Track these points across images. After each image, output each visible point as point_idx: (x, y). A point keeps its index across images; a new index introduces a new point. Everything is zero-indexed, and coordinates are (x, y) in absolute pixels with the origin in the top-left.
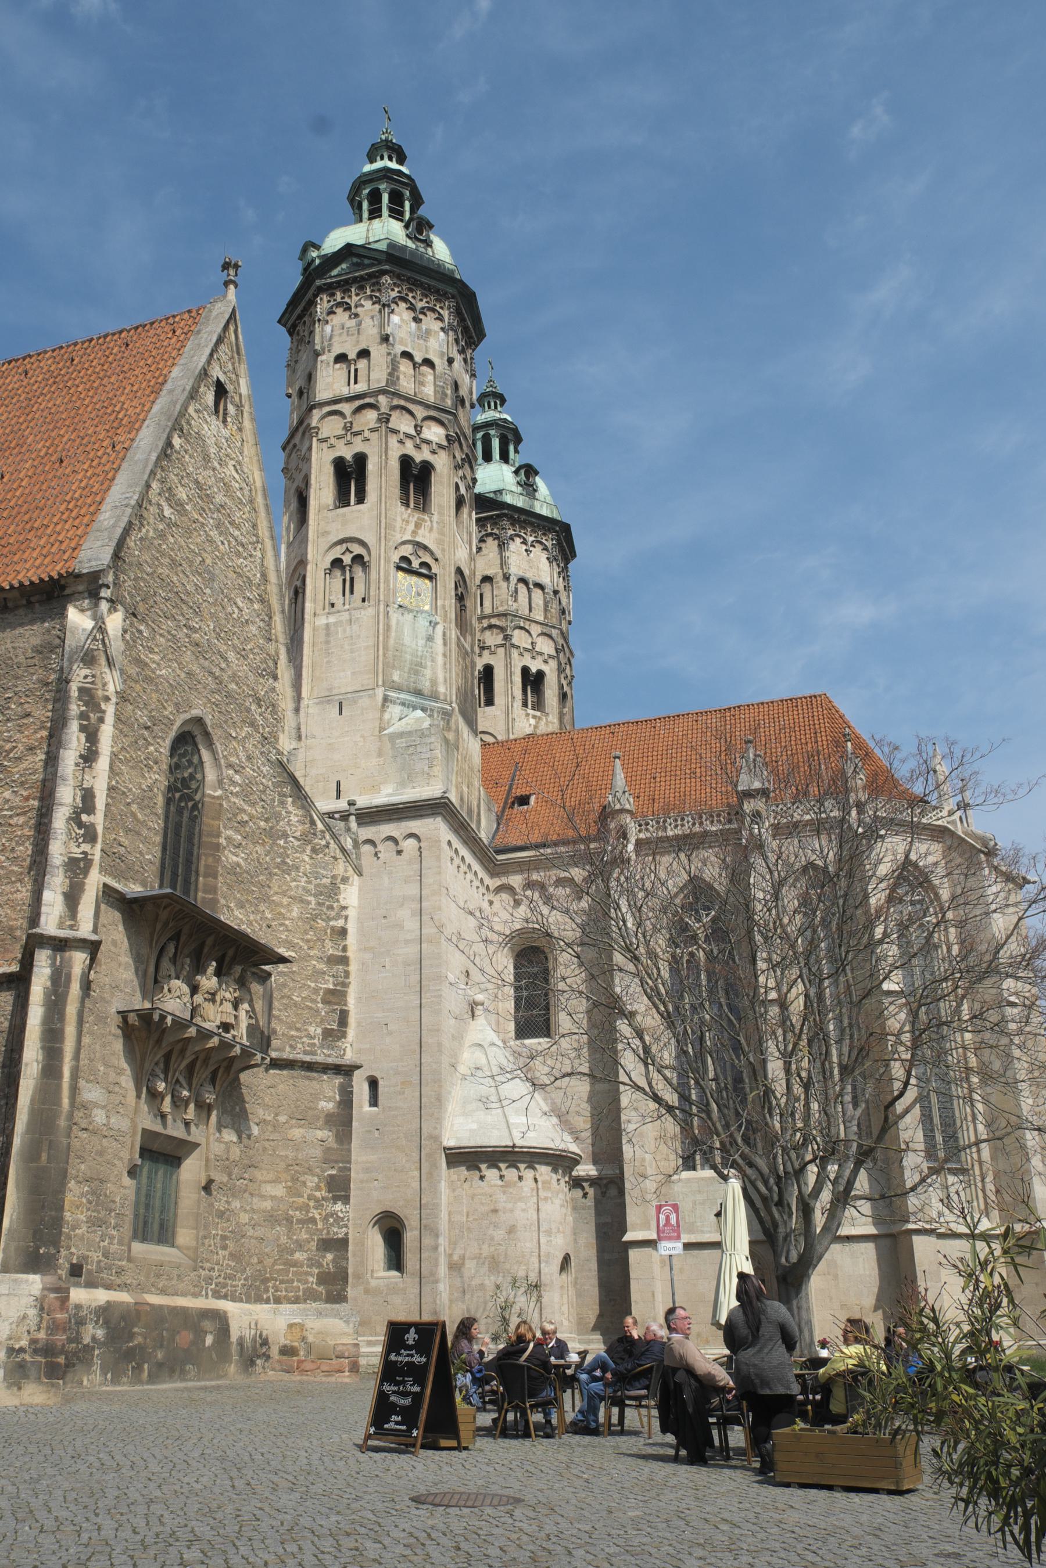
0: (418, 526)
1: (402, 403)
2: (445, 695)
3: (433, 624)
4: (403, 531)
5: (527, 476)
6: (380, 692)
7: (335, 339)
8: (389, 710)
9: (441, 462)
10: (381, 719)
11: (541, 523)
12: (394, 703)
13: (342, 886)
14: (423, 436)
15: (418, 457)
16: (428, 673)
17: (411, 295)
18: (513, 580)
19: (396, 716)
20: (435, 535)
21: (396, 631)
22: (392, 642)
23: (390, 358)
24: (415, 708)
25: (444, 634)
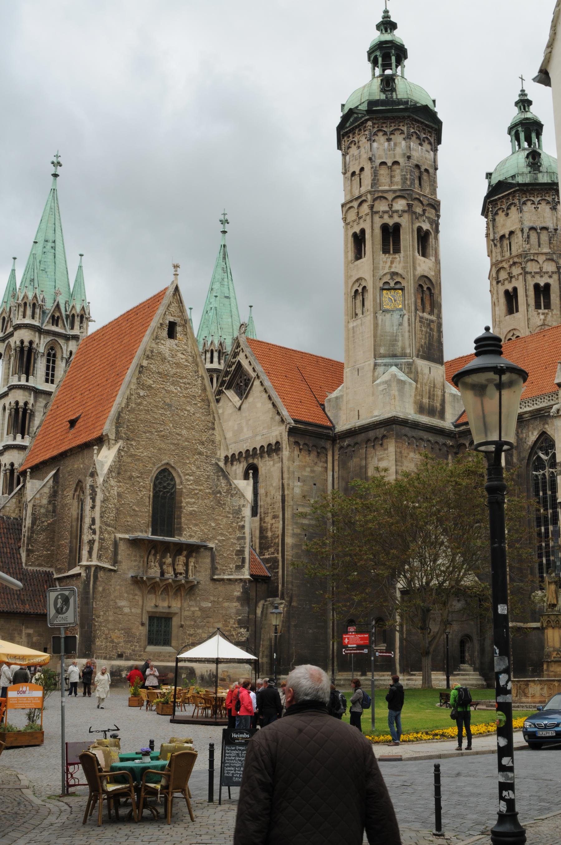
0: (392, 263)
1: (380, 194)
2: (410, 353)
3: (402, 316)
4: (384, 268)
5: (534, 158)
6: (372, 362)
7: (351, 163)
8: (377, 370)
9: (405, 221)
10: (373, 376)
11: (543, 187)
12: (380, 365)
13: (243, 509)
14: (394, 209)
15: (391, 222)
16: (400, 344)
17: (384, 125)
18: (526, 230)
19: (381, 373)
20: (402, 265)
21: (382, 325)
22: (379, 332)
23: (373, 169)
24: (391, 365)
25: (409, 320)
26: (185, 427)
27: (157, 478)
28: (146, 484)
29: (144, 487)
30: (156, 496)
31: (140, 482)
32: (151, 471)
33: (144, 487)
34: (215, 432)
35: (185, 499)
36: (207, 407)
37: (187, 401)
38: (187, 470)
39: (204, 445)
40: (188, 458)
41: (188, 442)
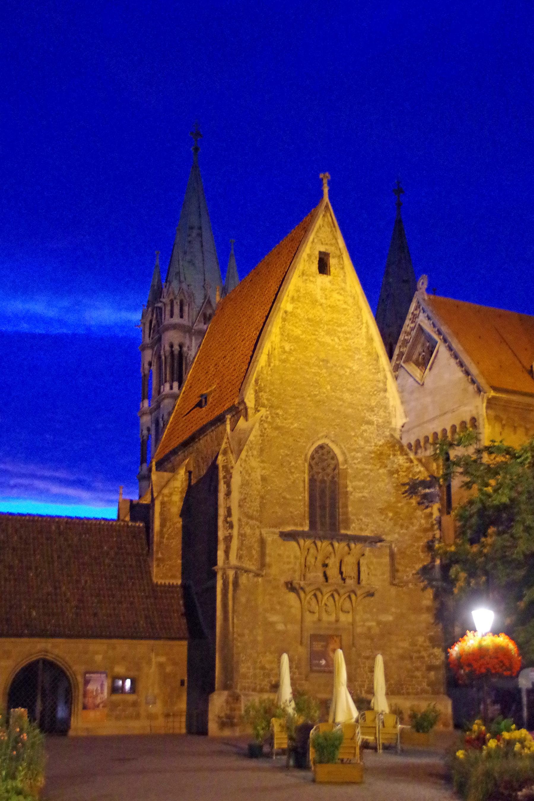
26: (348, 390)
27: (313, 458)
28: (299, 464)
29: (296, 468)
30: (312, 481)
31: (290, 463)
32: (305, 447)
33: (296, 468)
34: (387, 395)
35: (351, 482)
36: (375, 362)
37: (349, 356)
38: (352, 445)
39: (373, 411)
40: (353, 429)
41: (352, 408)
